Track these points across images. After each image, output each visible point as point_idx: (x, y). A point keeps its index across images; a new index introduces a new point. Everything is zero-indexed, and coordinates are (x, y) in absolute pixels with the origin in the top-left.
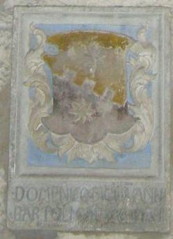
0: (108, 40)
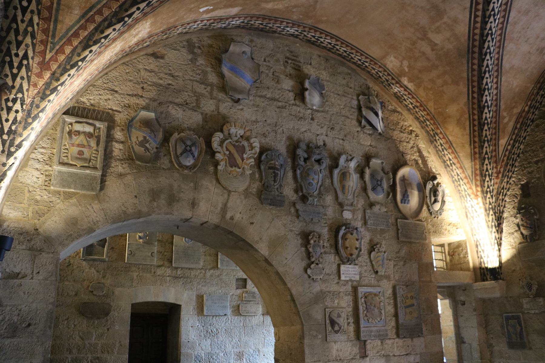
0: (376, 295)
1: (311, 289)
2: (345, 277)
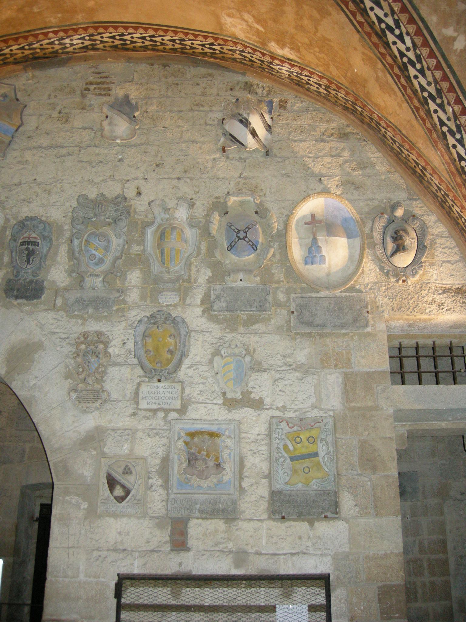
0: (212, 435)
2: (148, 404)
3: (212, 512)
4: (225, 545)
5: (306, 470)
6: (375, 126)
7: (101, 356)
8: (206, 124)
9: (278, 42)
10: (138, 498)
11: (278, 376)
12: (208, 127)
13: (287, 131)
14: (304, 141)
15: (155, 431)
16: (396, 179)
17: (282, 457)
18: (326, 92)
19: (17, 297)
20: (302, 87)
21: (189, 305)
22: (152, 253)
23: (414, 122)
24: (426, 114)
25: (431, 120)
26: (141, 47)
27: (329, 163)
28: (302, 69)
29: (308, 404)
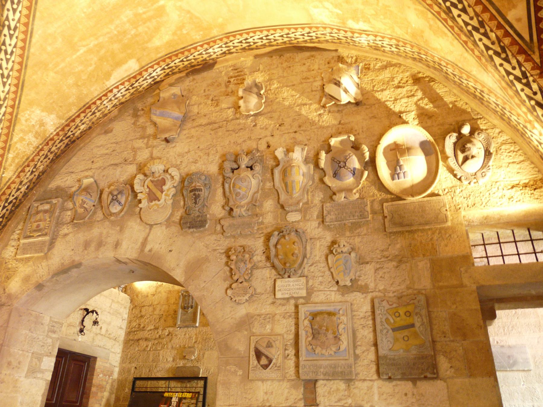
0: (330, 314)
1: (233, 313)
2: (282, 294)
3: (334, 374)
4: (345, 401)
5: (406, 339)
6: (438, 67)
7: (247, 262)
8: (312, 91)
9: (353, 19)
10: (278, 365)
11: (378, 266)
12: (314, 93)
13: (372, 85)
14: (385, 90)
15: (288, 314)
16: (462, 105)
17: (386, 328)
18: (397, 50)
19: (189, 228)
20: (379, 50)
21: (308, 220)
22: (279, 186)
23: (466, 55)
24: (473, 45)
25: (478, 48)
26: (261, 45)
27: (406, 103)
28: (376, 36)
29: (403, 287)
